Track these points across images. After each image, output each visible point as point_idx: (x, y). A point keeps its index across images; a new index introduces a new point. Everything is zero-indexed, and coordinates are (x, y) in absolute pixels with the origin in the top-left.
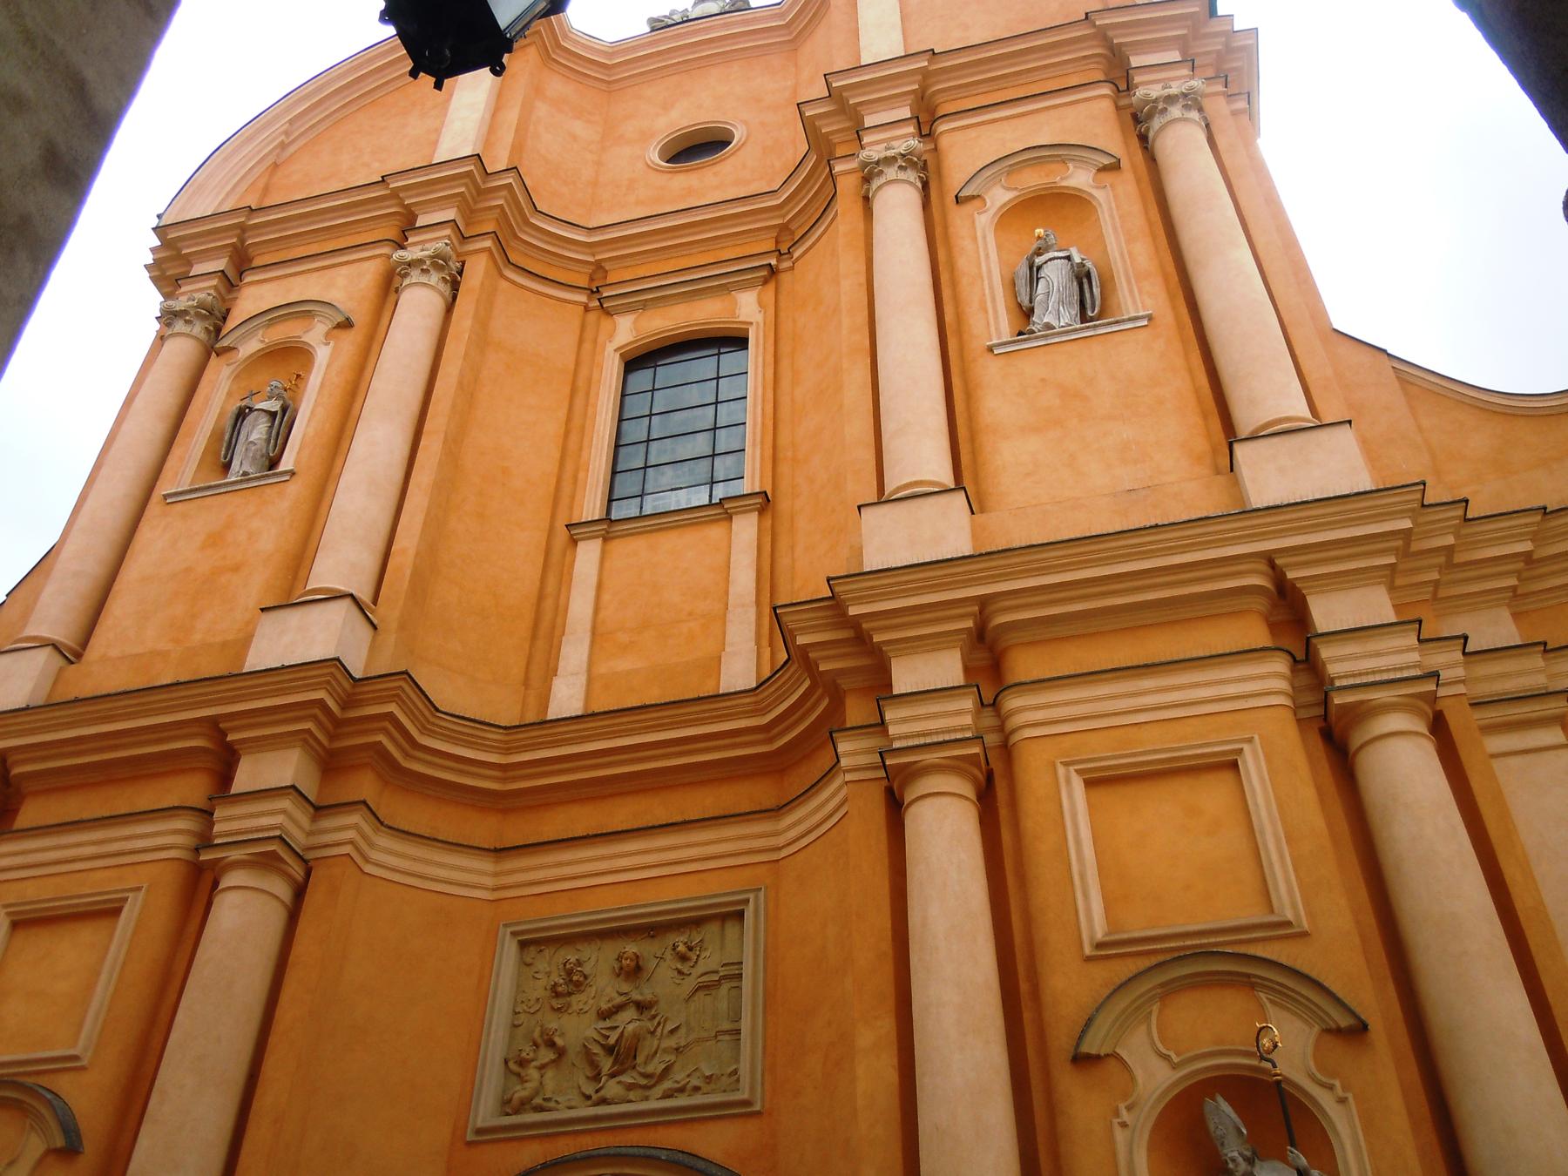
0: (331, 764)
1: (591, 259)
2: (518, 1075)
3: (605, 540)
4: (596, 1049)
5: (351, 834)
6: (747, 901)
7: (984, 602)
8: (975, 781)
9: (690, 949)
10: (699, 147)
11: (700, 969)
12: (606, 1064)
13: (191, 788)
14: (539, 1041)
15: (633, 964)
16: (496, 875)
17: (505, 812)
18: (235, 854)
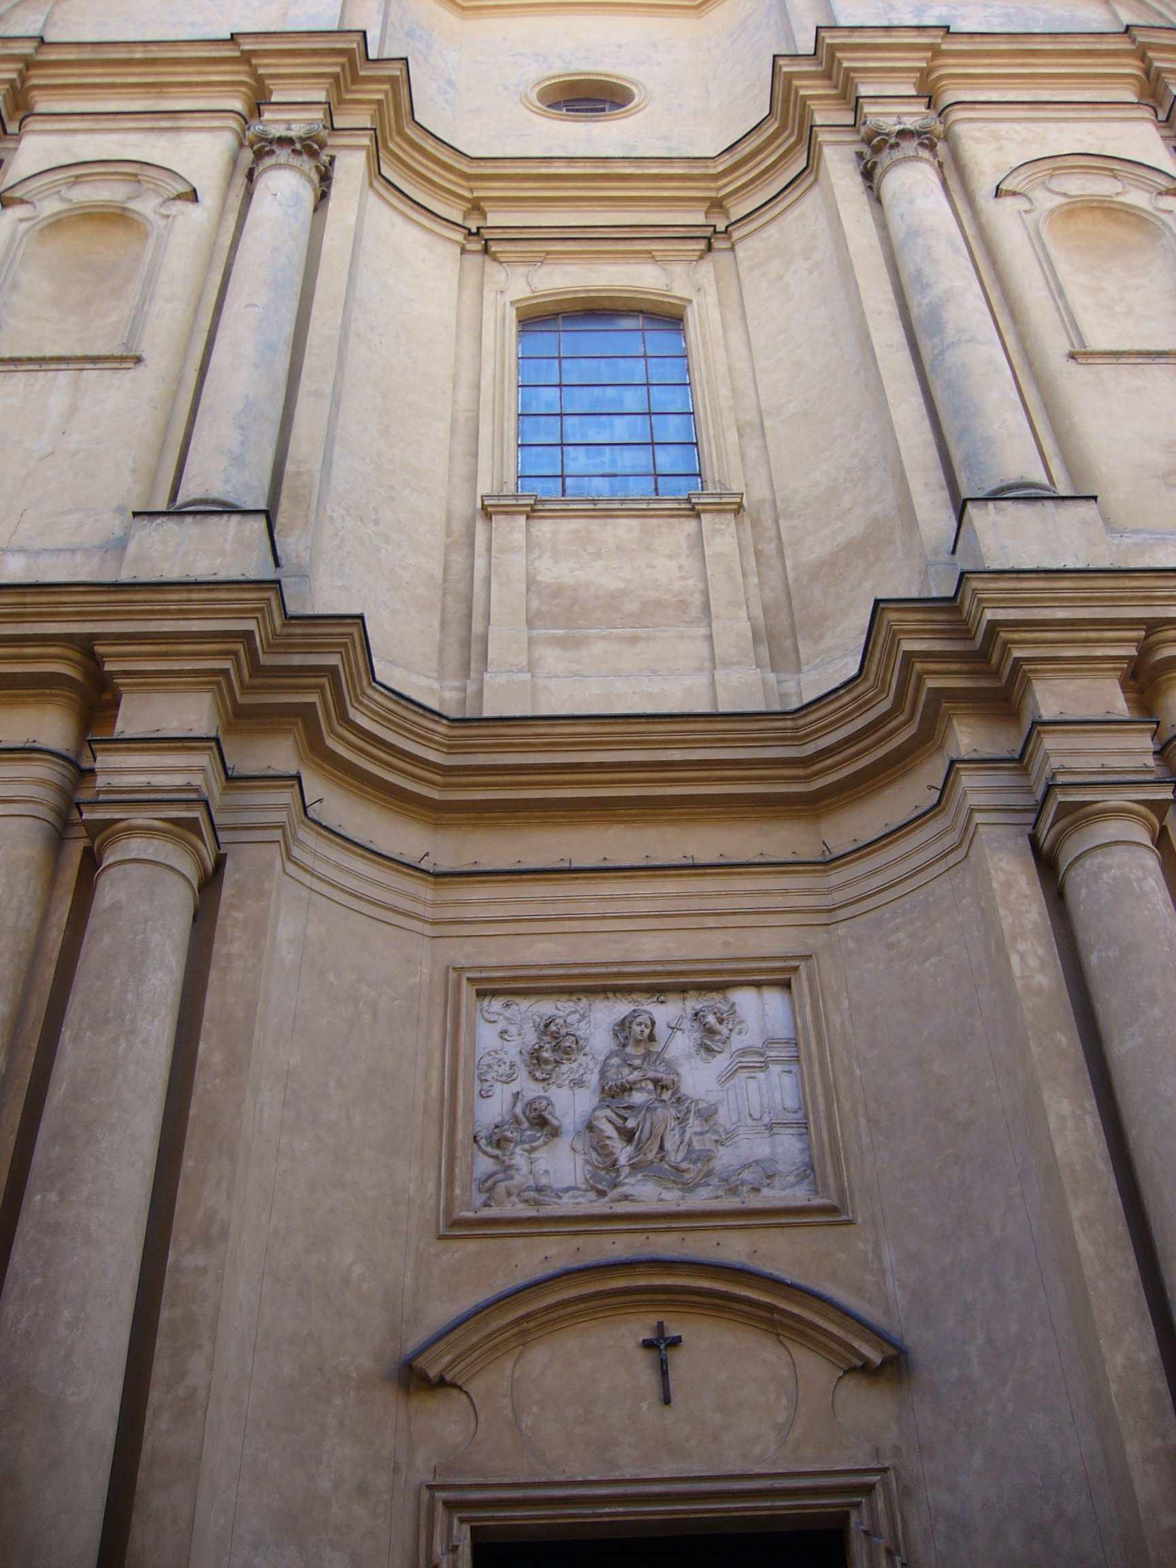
0: (243, 718)
1: (466, 194)
2: (496, 1157)
3: (528, 518)
4: (609, 1130)
5: (281, 817)
6: (796, 969)
7: (1153, 625)
8: (1152, 831)
9: (721, 1021)
10: (588, 97)
11: (737, 1042)
12: (624, 1153)
13: (49, 725)
14: (521, 1116)
15: (647, 1031)
16: (435, 905)
17: (437, 825)
18: (140, 818)
